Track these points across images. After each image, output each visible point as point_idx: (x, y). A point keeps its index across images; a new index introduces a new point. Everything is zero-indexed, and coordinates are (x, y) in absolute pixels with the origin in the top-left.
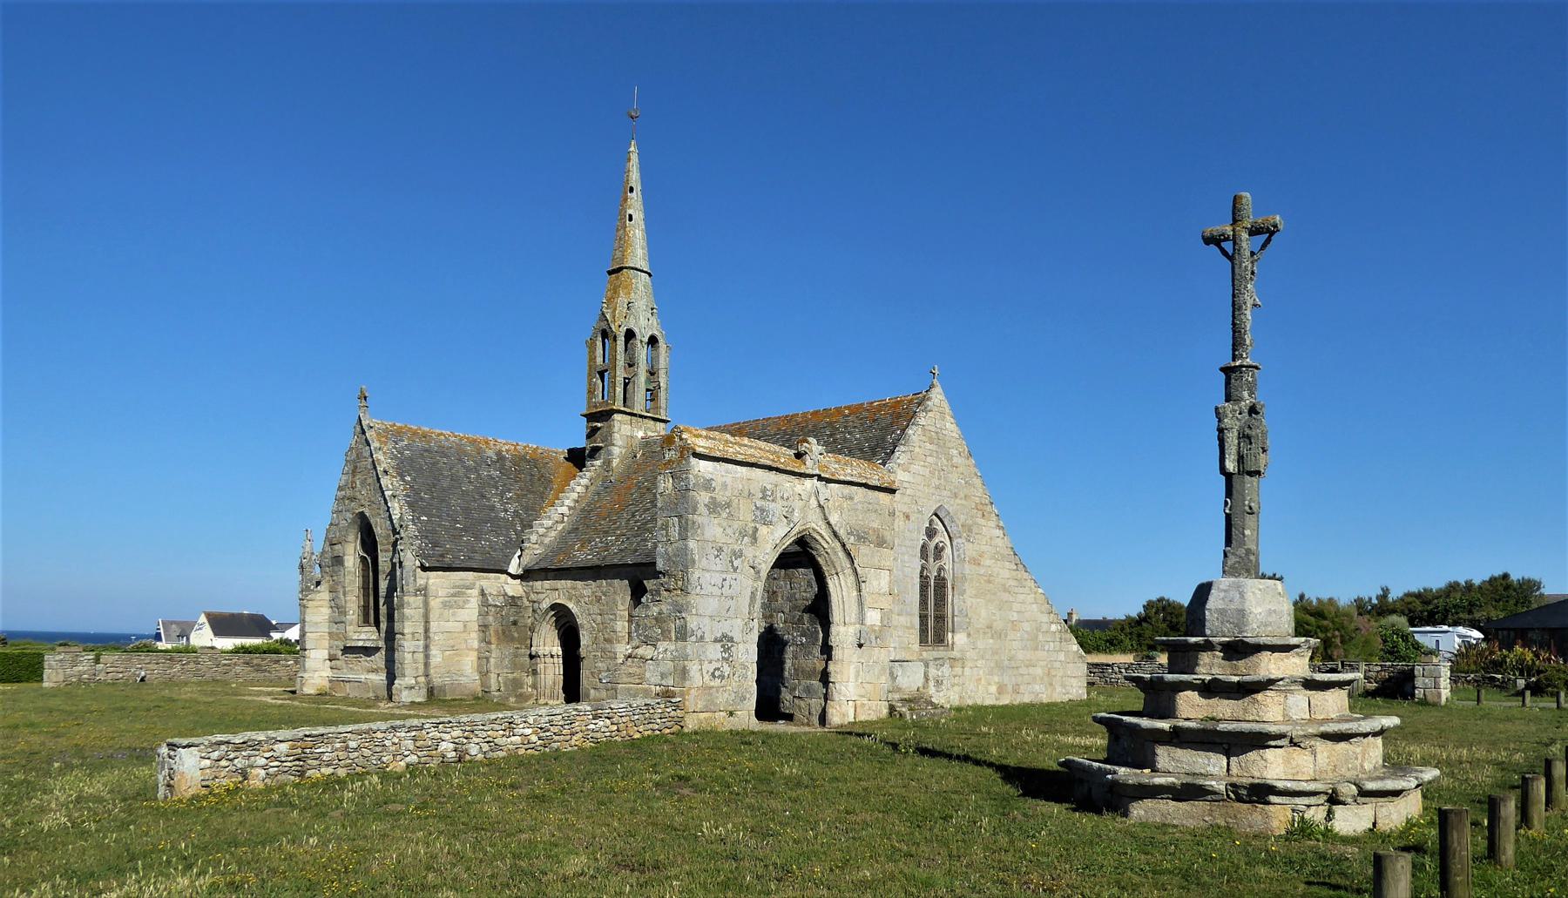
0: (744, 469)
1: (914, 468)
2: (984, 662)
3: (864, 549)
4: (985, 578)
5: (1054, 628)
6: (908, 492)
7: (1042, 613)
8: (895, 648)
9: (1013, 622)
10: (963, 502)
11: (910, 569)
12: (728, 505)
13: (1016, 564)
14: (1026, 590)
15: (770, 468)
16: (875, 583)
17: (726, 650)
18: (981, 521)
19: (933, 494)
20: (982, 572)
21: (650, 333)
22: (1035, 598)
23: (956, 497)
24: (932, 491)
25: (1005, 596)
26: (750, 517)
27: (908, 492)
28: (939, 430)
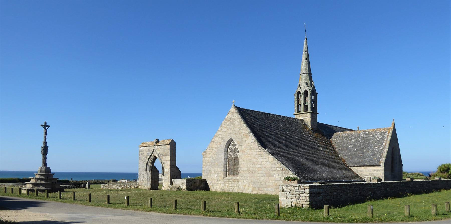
0: (145, 147)
1: (223, 130)
2: (246, 180)
3: (164, 157)
4: (246, 156)
5: (278, 169)
6: (221, 137)
7: (272, 164)
8: (216, 176)
9: (258, 168)
10: (238, 135)
11: (221, 156)
12: (143, 154)
13: (260, 150)
14: (264, 157)
15: (149, 146)
16: (166, 163)
17: (143, 176)
18: (245, 139)
19: (228, 136)
20: (245, 154)
21: (304, 90)
22: (268, 160)
23: (236, 134)
24: (228, 135)
25: (255, 160)
26: (146, 155)
27: (221, 137)
28: (231, 118)
